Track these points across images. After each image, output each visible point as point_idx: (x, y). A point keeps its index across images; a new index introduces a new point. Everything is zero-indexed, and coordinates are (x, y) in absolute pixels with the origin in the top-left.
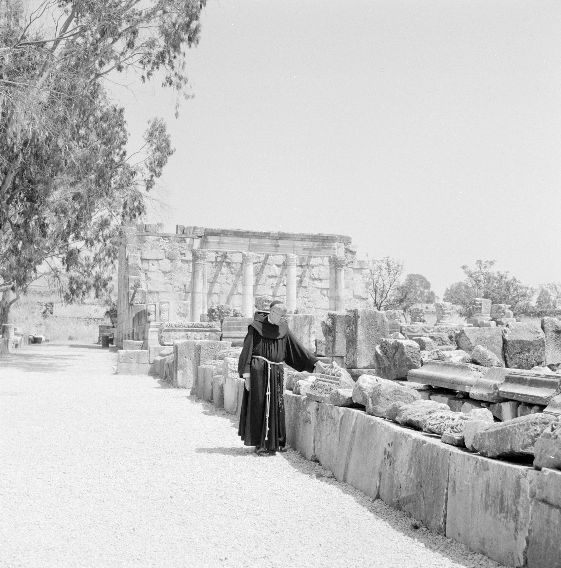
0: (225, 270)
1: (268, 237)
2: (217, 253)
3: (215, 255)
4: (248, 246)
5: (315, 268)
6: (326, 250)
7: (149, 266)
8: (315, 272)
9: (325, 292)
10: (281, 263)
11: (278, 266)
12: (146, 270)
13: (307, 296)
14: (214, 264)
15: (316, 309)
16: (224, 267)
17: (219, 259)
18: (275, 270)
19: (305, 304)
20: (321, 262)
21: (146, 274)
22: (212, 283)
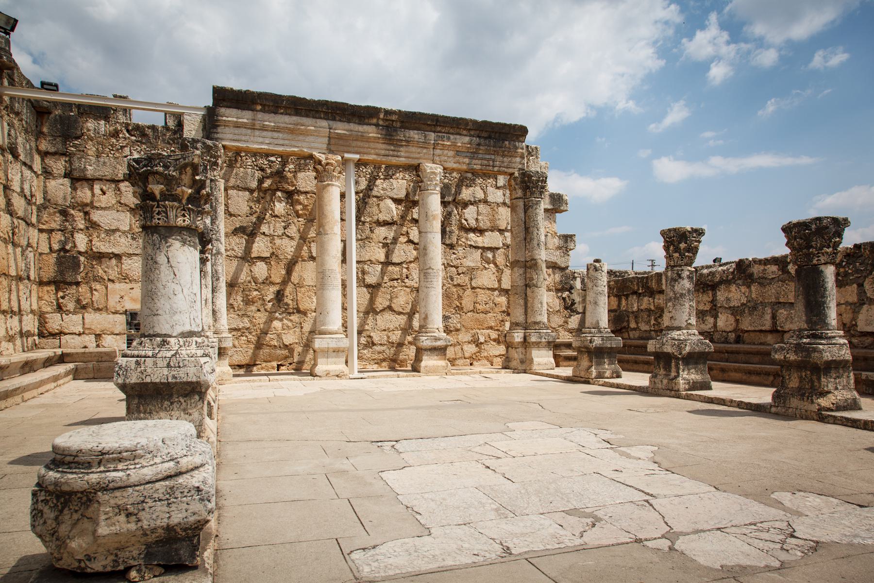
0: (280, 207)
1: (375, 121)
2: (262, 170)
3: (258, 174)
4: (326, 140)
5: (471, 207)
6: (505, 159)
7: (93, 195)
8: (470, 213)
9: (490, 255)
10: (402, 195)
11: (397, 201)
12: (87, 205)
13: (455, 263)
14: (256, 194)
15: (473, 288)
16: (280, 201)
17: (267, 184)
18: (389, 210)
19: (452, 279)
20: (480, 195)
21: (86, 213)
22: (250, 233)
